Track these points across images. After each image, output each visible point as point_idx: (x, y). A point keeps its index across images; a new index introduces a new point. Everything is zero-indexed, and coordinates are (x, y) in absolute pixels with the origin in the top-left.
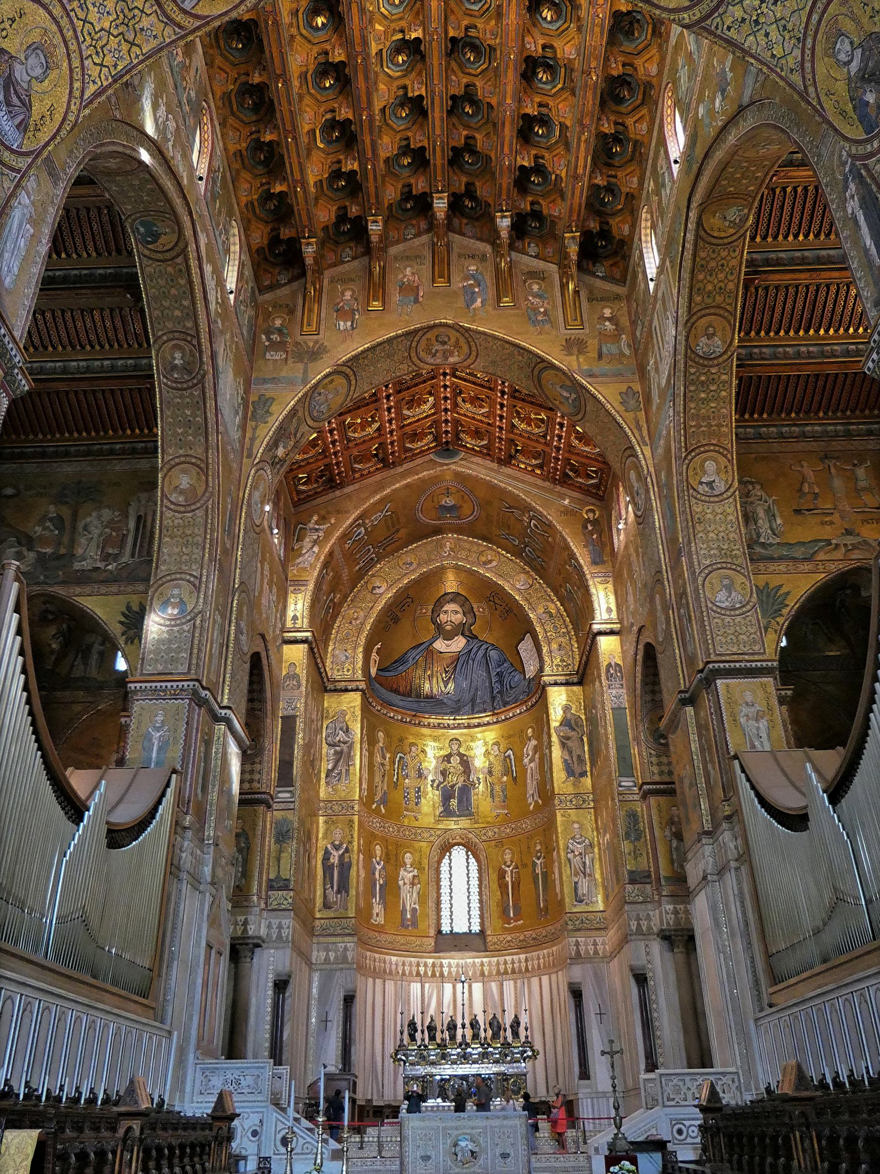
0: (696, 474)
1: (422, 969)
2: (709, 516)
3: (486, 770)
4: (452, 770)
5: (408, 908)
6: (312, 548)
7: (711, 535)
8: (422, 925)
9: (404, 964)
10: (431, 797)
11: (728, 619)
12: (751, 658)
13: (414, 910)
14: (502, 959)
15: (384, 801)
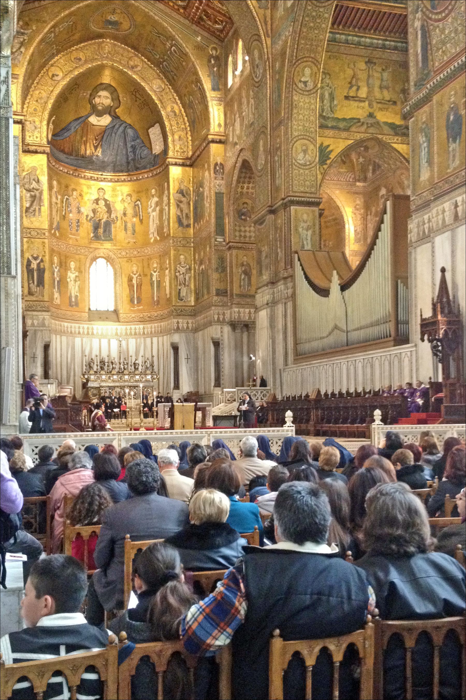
0: (299, 75)
1: (81, 331)
2: (301, 104)
3: (122, 212)
4: (99, 210)
5: (73, 295)
6: (20, 48)
7: (301, 116)
8: (80, 305)
9: (71, 327)
10: (87, 227)
11: (302, 171)
12: (310, 195)
13: (76, 296)
14: (129, 327)
15: (58, 228)
